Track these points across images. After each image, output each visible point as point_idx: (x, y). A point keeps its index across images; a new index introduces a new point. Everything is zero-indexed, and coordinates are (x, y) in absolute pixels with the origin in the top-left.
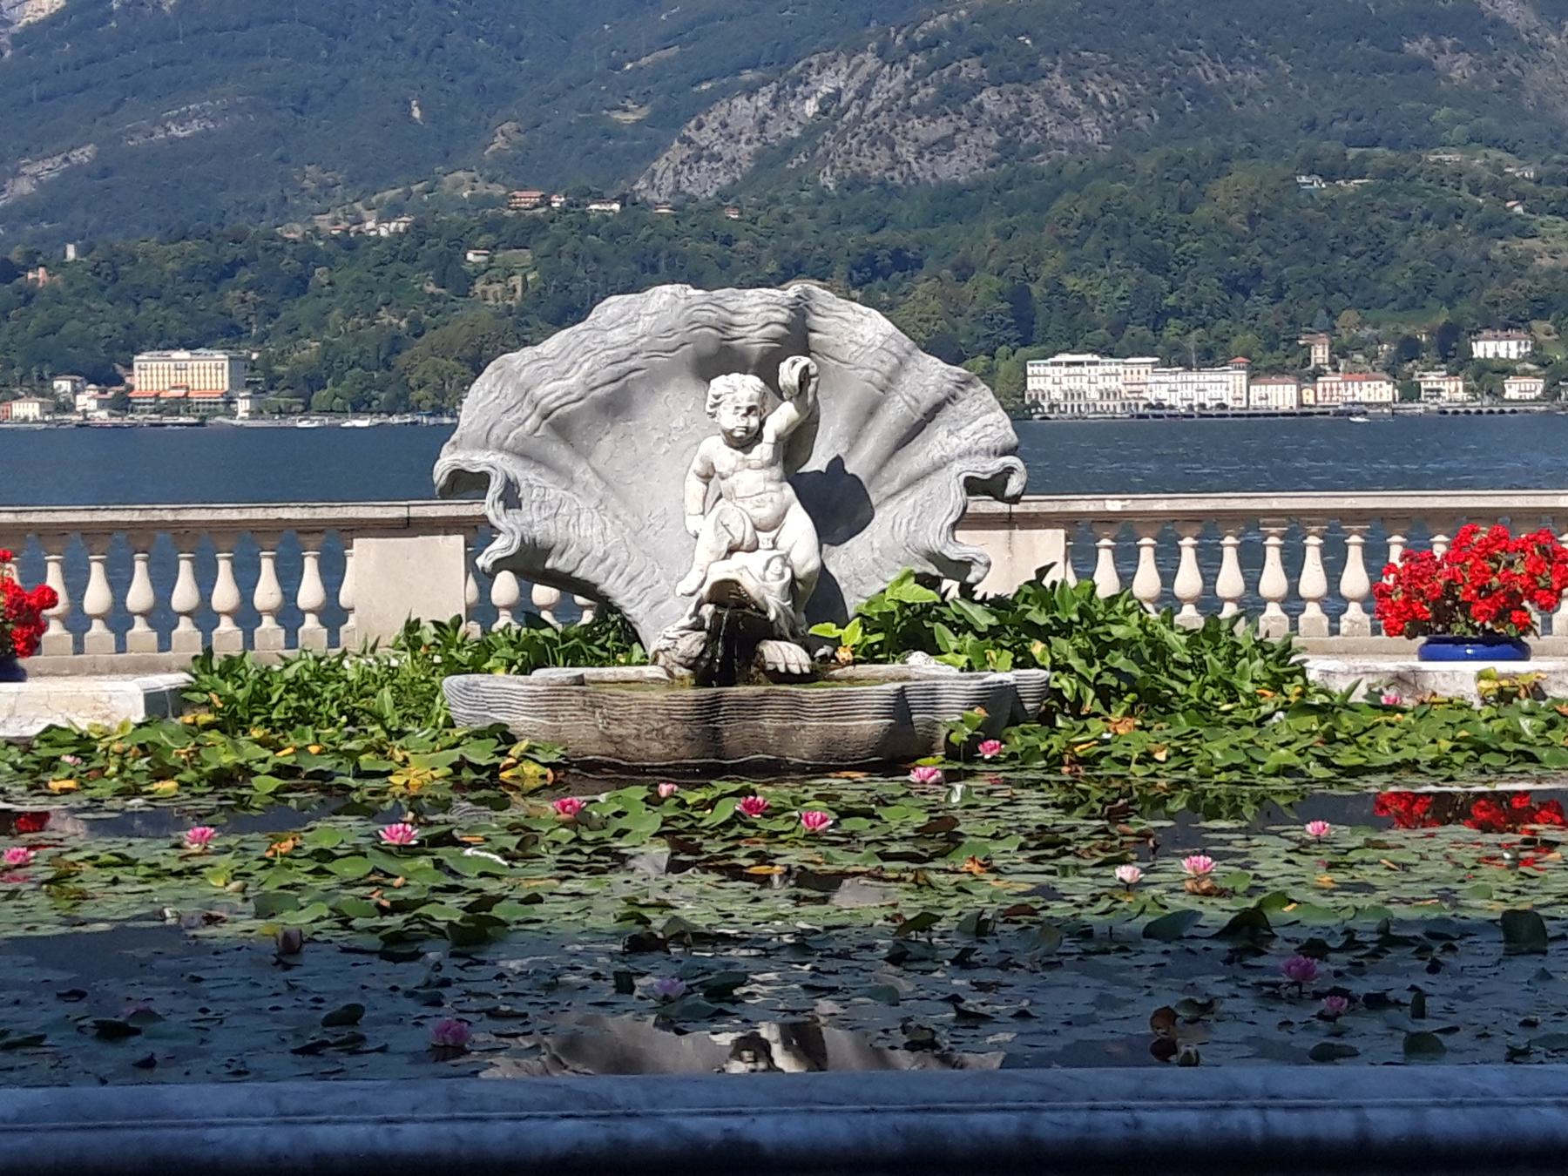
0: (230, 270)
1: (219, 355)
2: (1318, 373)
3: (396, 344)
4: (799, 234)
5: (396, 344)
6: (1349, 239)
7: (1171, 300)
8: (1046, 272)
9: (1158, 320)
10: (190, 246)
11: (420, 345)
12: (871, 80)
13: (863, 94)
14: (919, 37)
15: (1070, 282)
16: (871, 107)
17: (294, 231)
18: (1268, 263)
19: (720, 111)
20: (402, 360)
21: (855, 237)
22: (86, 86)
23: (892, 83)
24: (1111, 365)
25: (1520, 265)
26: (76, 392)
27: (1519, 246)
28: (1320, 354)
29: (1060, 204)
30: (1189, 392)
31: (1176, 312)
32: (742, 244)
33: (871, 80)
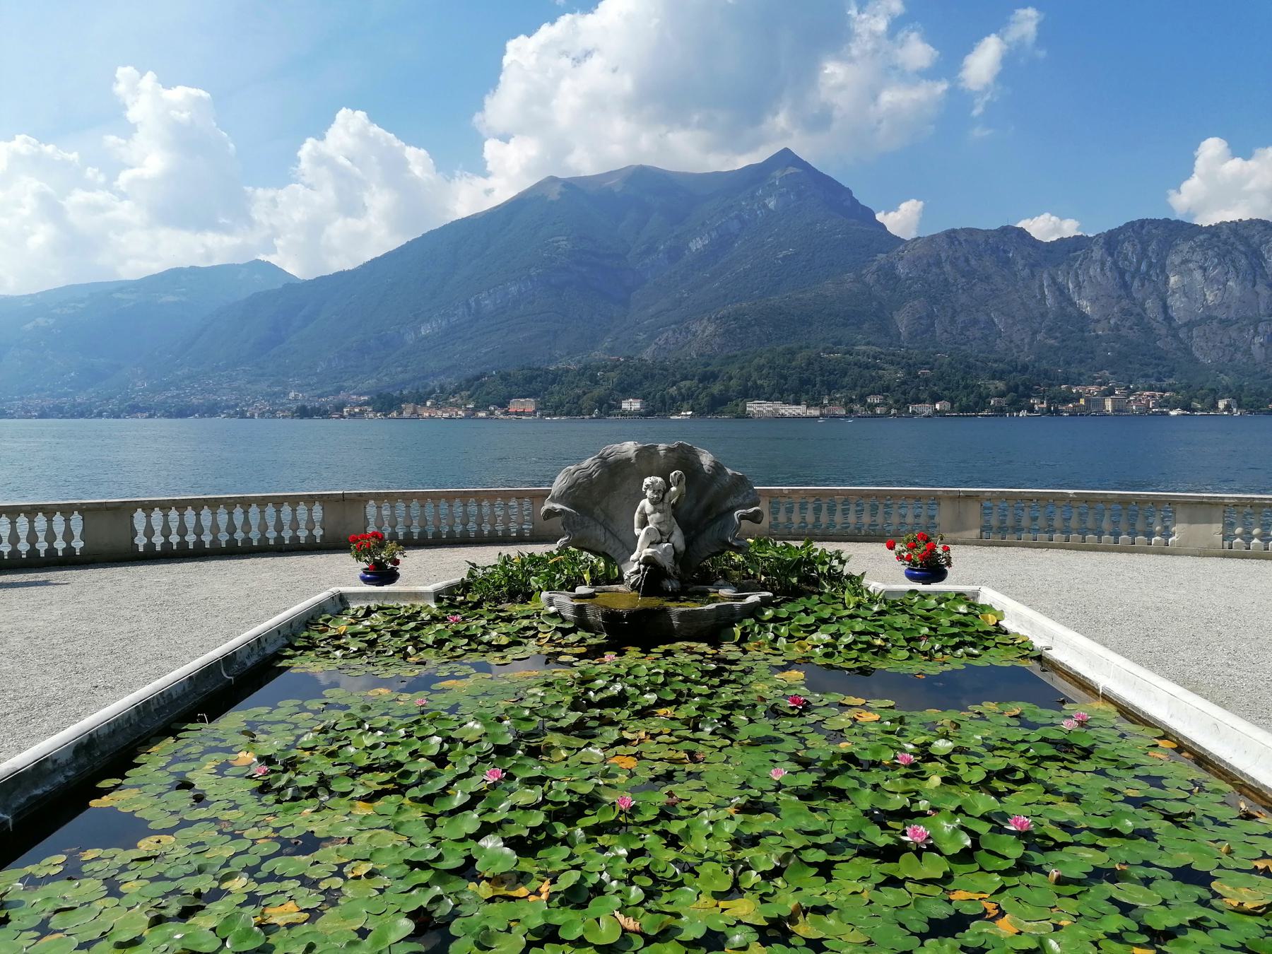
0: (535, 378)
1: (532, 400)
2: (825, 406)
3: (579, 397)
4: (686, 369)
5: (579, 397)
6: (835, 370)
7: (786, 386)
8: (753, 379)
9: (782, 393)
10: (525, 372)
11: (585, 398)
12: (706, 327)
13: (704, 332)
14: (719, 316)
15: (759, 382)
16: (706, 334)
17: (552, 368)
18: (812, 377)
19: (665, 335)
20: (580, 402)
21: (701, 369)
22: (499, 330)
23: (710, 329)
24: (770, 404)
25: (880, 378)
26: (495, 410)
27: (881, 372)
28: (825, 402)
29: (756, 361)
30: (790, 411)
31: (787, 390)
32: (671, 371)
33: (706, 327)
